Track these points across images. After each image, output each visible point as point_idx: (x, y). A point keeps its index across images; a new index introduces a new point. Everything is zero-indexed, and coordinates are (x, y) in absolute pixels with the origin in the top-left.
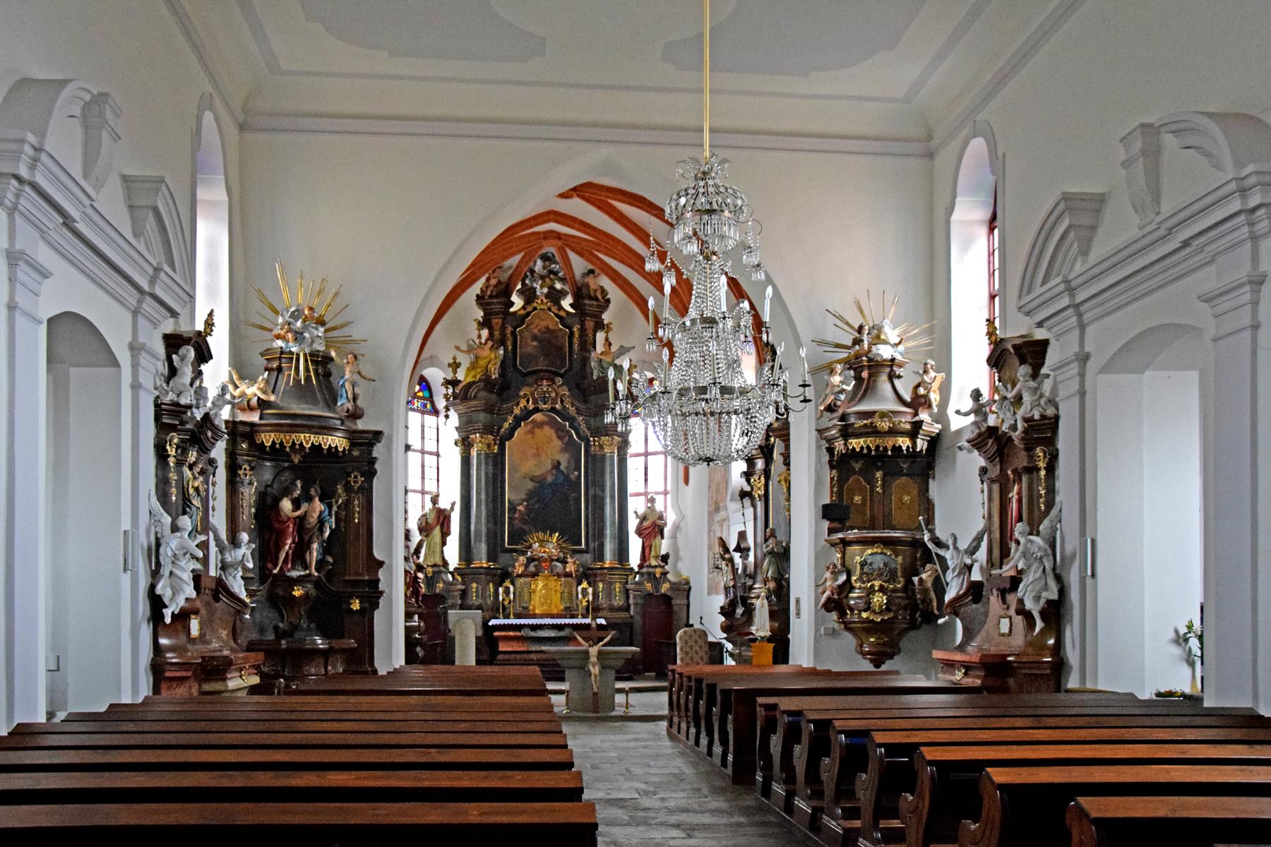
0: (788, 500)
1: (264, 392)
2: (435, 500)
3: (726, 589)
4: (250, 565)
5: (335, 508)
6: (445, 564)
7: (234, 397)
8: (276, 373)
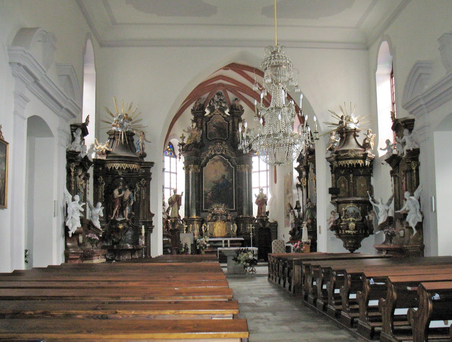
0: (316, 187)
1: (108, 147)
2: (175, 191)
3: (292, 224)
4: (102, 215)
5: (135, 193)
6: (179, 217)
7: (96, 149)
8: (113, 140)
